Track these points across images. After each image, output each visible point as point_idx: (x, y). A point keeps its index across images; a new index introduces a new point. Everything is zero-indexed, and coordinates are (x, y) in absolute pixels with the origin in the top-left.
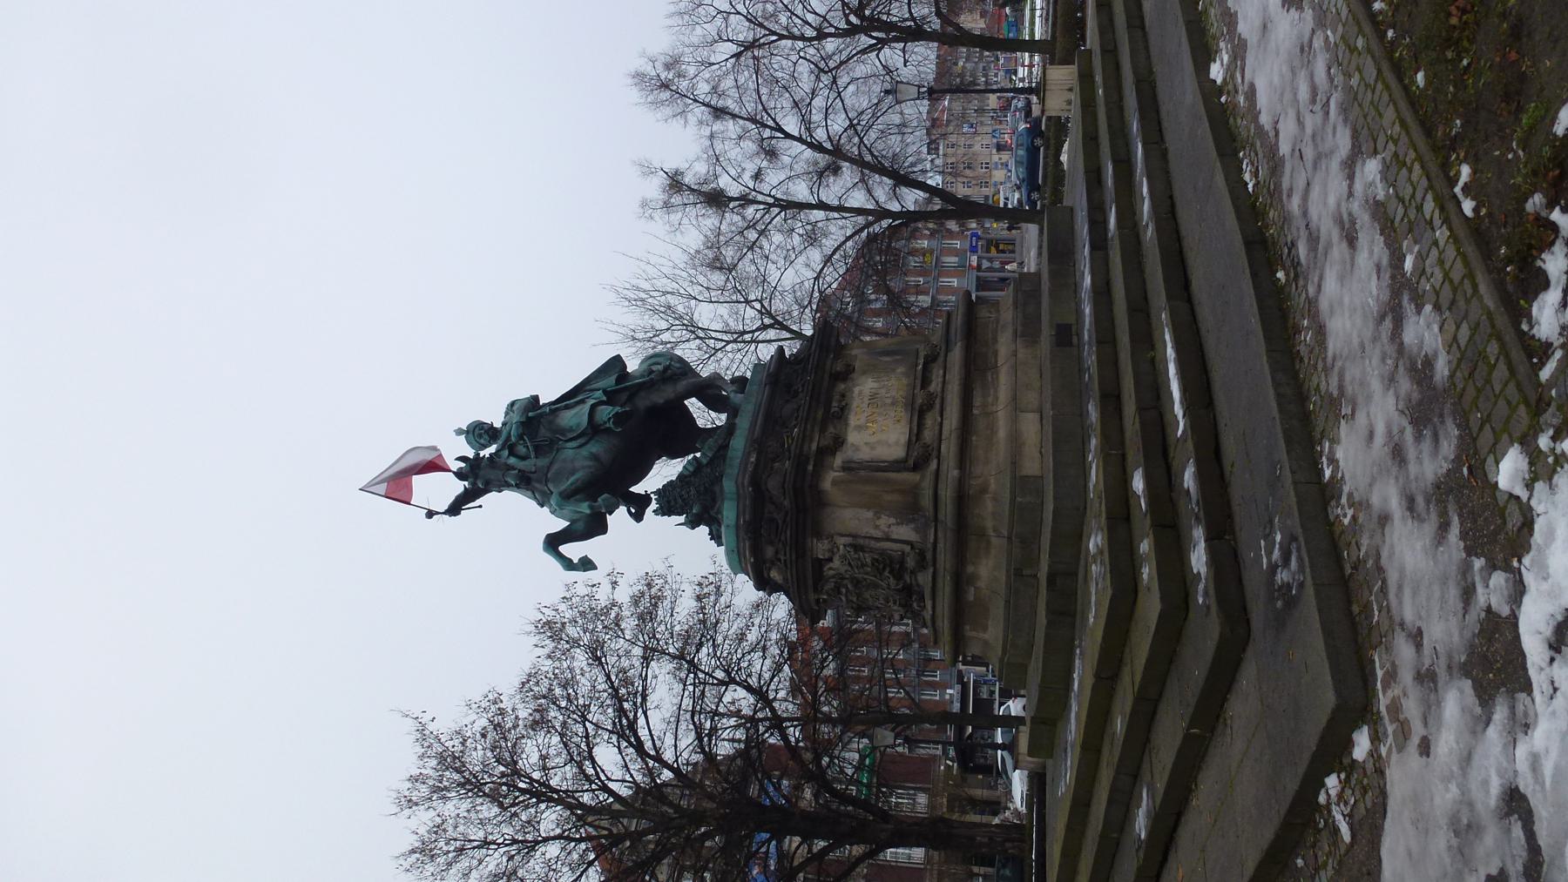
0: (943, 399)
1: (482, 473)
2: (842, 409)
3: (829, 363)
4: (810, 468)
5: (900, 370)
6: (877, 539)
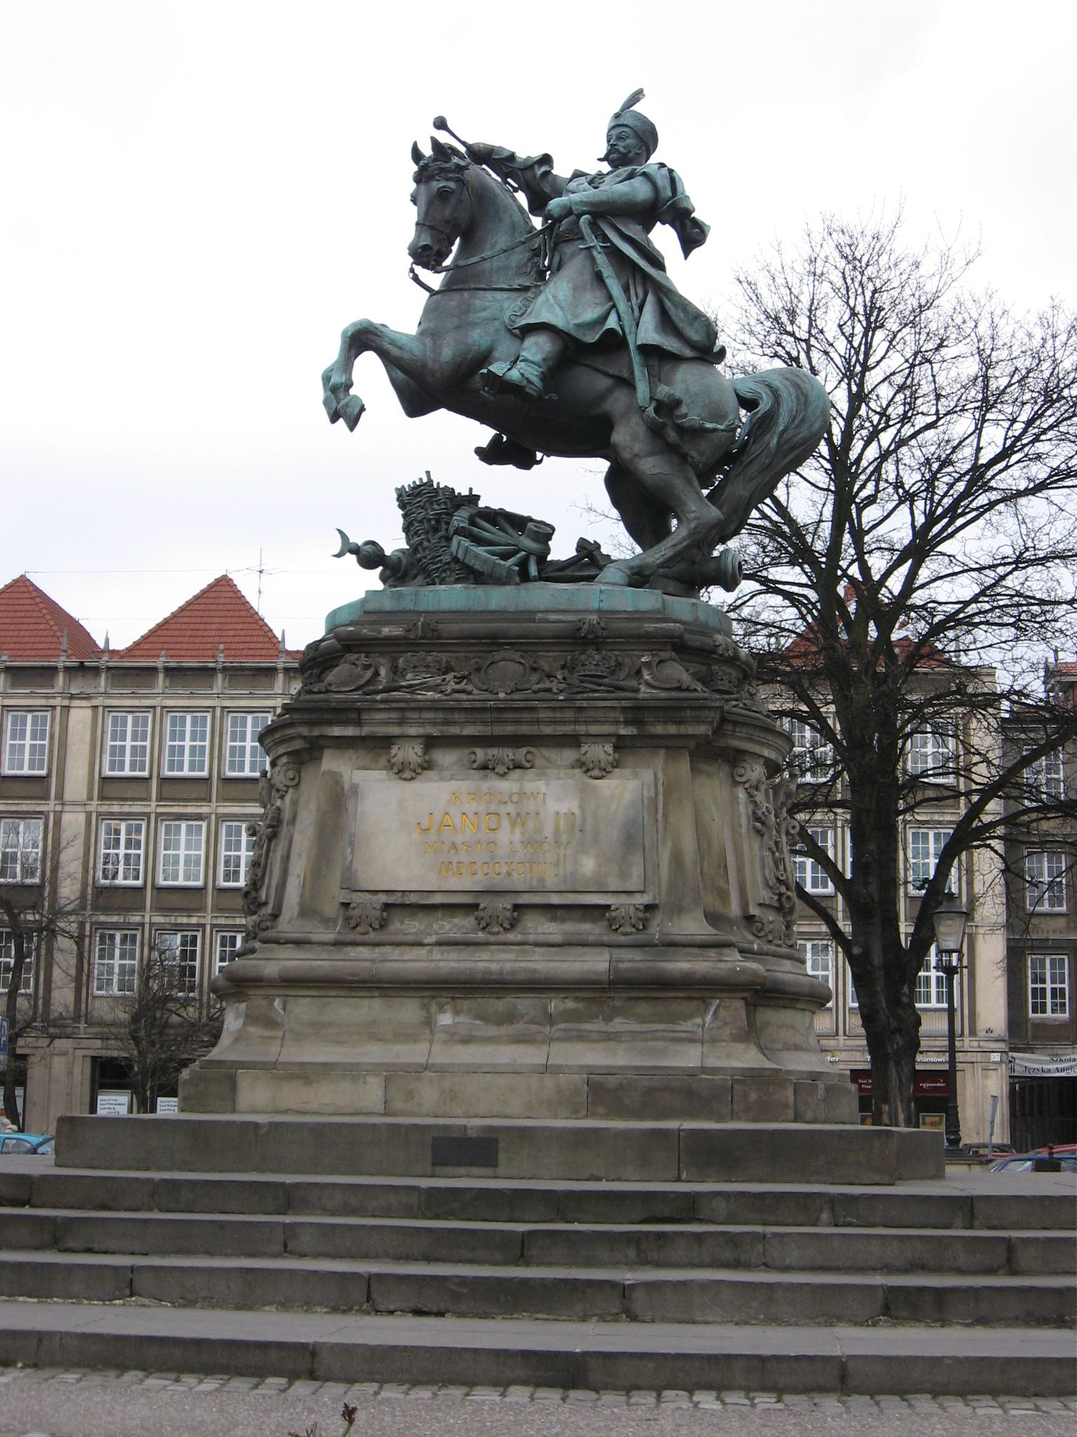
0: (487, 944)
1: (423, 187)
2: (484, 767)
3: (594, 729)
4: (337, 731)
5: (589, 865)
6: (286, 859)
